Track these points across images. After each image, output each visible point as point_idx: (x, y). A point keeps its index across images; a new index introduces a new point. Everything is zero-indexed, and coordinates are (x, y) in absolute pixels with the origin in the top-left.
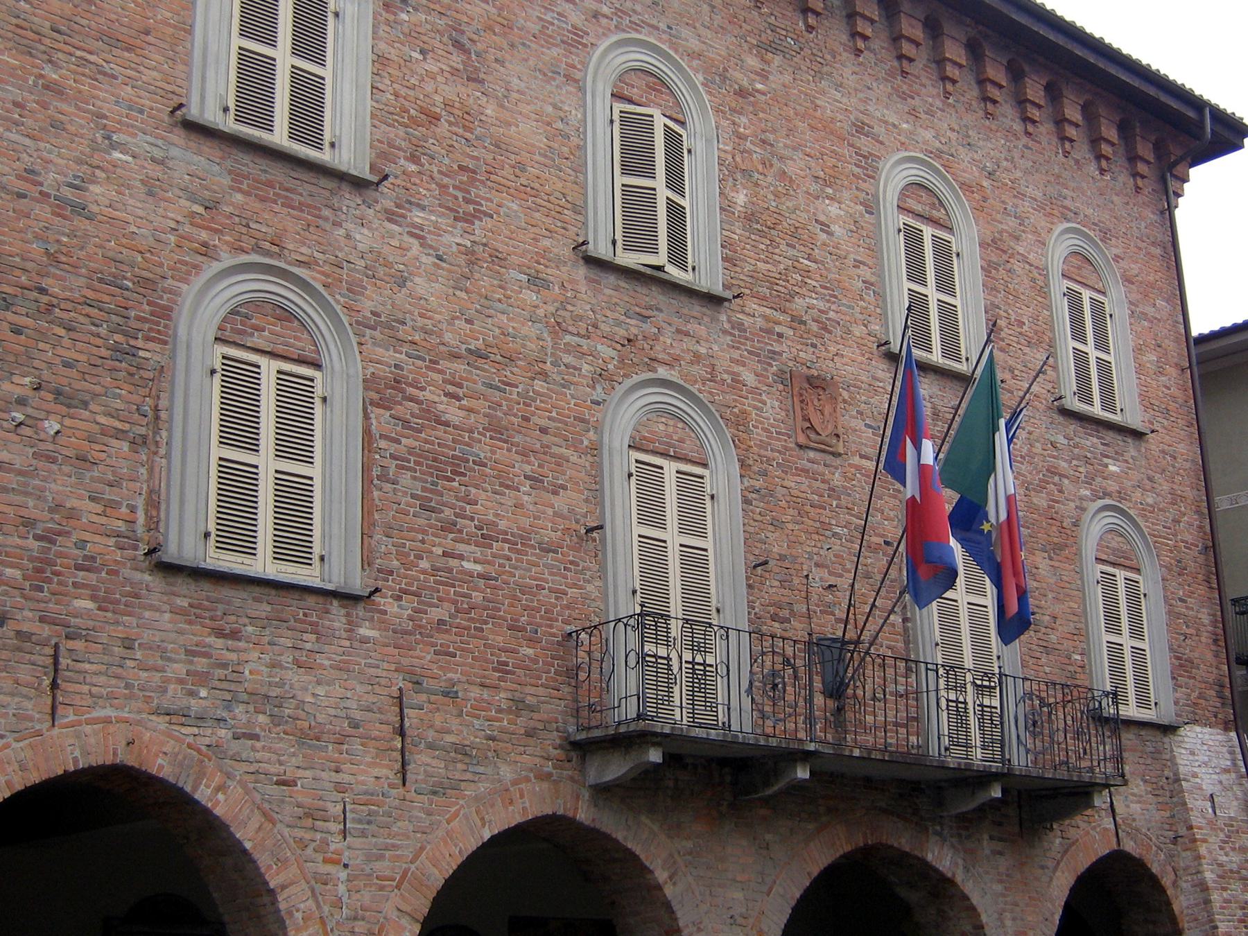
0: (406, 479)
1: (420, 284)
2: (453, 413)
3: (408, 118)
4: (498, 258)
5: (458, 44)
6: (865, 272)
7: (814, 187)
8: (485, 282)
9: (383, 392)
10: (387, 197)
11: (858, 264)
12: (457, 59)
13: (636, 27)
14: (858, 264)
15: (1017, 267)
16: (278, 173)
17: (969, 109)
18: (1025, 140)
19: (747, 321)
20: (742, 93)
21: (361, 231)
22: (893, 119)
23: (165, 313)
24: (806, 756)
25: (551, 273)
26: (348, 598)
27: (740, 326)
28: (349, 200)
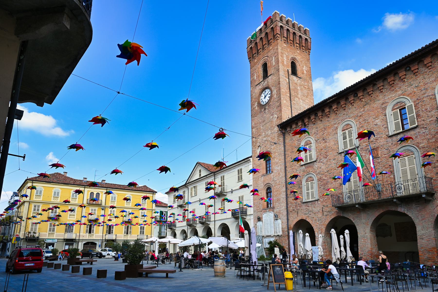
0: (322, 187)
1: (322, 167)
2: (326, 178)
3: (319, 151)
4: (330, 159)
5: (324, 140)
6: (385, 126)
7: (373, 120)
8: (328, 163)
9: (319, 180)
10: (318, 161)
11: (383, 126)
12: (324, 141)
13: (344, 120)
14: (383, 126)
15: (425, 99)
16: (309, 165)
17: (412, 78)
18: (429, 70)
19: (363, 147)
20: (361, 116)
21: (316, 165)
22: (391, 96)
23: (302, 182)
24: (356, 204)
25: (336, 158)
26: (317, 200)
27: (362, 148)
28: (315, 163)
